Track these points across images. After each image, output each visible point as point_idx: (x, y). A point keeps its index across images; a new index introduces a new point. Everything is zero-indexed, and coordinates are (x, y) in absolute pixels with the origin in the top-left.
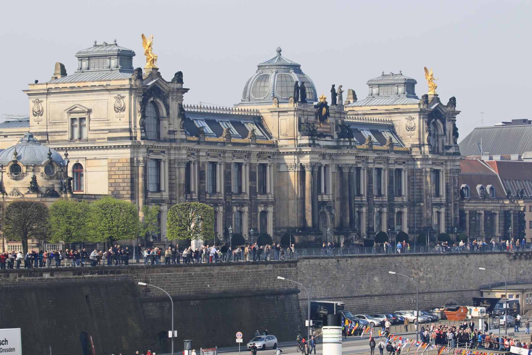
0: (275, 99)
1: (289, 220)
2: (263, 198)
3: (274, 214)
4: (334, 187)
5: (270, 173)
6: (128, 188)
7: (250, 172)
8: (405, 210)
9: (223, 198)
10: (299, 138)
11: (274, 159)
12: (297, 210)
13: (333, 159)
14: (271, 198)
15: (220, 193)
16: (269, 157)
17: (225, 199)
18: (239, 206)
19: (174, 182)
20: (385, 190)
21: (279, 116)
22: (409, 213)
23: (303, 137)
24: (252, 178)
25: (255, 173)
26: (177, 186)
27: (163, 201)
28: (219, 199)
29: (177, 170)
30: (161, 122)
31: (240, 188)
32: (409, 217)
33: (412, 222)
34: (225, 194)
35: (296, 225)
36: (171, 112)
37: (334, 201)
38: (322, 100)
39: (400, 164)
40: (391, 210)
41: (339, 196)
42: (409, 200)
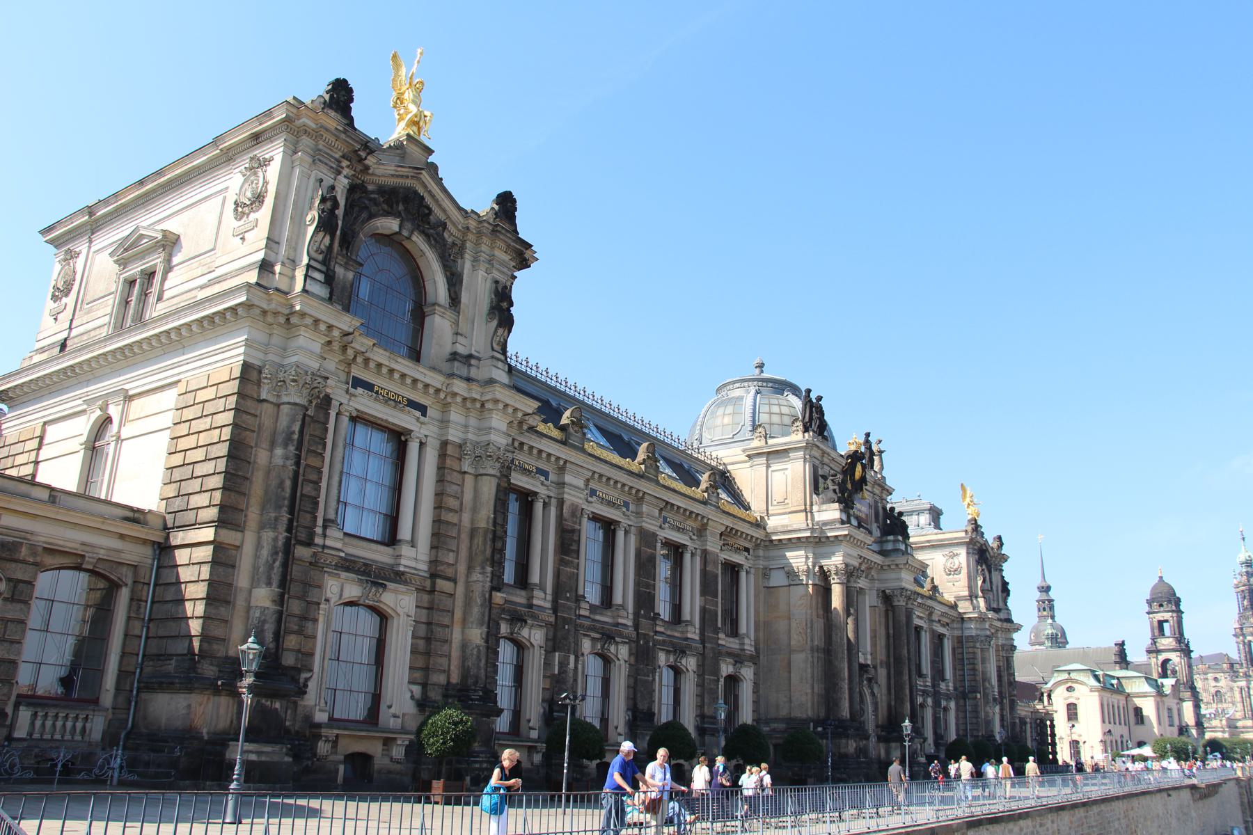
0: (759, 430)
1: (790, 701)
2: (733, 644)
3: (756, 685)
4: (874, 637)
5: (747, 586)
6: (217, 481)
7: (704, 573)
8: (952, 705)
9: (630, 623)
10: (815, 508)
11: (757, 557)
12: (813, 677)
13: (873, 579)
14: (749, 647)
15: (623, 607)
16: (747, 550)
17: (636, 626)
18: (675, 652)
19: (451, 517)
20: (926, 668)
21: (768, 467)
22: (957, 710)
23: (824, 507)
24: (707, 587)
25: (716, 576)
26: (465, 537)
27: (398, 576)
28: (618, 624)
29: (469, 480)
30: (427, 320)
31: (677, 609)
32: (957, 718)
33: (962, 727)
34: (637, 615)
35: (810, 713)
36: (464, 298)
37: (875, 667)
38: (853, 448)
39: (943, 626)
40: (937, 704)
41: (884, 658)
42: (955, 689)
